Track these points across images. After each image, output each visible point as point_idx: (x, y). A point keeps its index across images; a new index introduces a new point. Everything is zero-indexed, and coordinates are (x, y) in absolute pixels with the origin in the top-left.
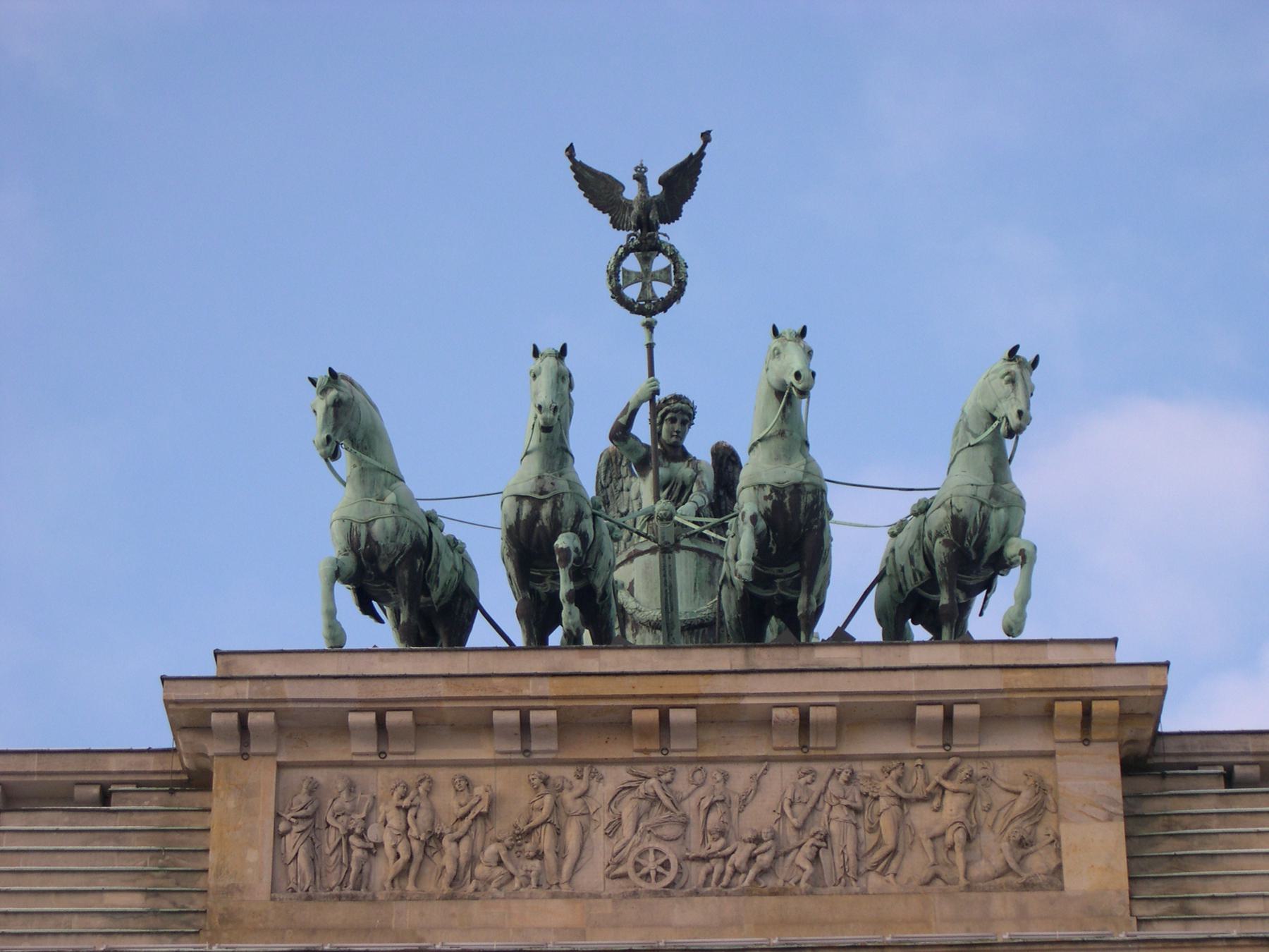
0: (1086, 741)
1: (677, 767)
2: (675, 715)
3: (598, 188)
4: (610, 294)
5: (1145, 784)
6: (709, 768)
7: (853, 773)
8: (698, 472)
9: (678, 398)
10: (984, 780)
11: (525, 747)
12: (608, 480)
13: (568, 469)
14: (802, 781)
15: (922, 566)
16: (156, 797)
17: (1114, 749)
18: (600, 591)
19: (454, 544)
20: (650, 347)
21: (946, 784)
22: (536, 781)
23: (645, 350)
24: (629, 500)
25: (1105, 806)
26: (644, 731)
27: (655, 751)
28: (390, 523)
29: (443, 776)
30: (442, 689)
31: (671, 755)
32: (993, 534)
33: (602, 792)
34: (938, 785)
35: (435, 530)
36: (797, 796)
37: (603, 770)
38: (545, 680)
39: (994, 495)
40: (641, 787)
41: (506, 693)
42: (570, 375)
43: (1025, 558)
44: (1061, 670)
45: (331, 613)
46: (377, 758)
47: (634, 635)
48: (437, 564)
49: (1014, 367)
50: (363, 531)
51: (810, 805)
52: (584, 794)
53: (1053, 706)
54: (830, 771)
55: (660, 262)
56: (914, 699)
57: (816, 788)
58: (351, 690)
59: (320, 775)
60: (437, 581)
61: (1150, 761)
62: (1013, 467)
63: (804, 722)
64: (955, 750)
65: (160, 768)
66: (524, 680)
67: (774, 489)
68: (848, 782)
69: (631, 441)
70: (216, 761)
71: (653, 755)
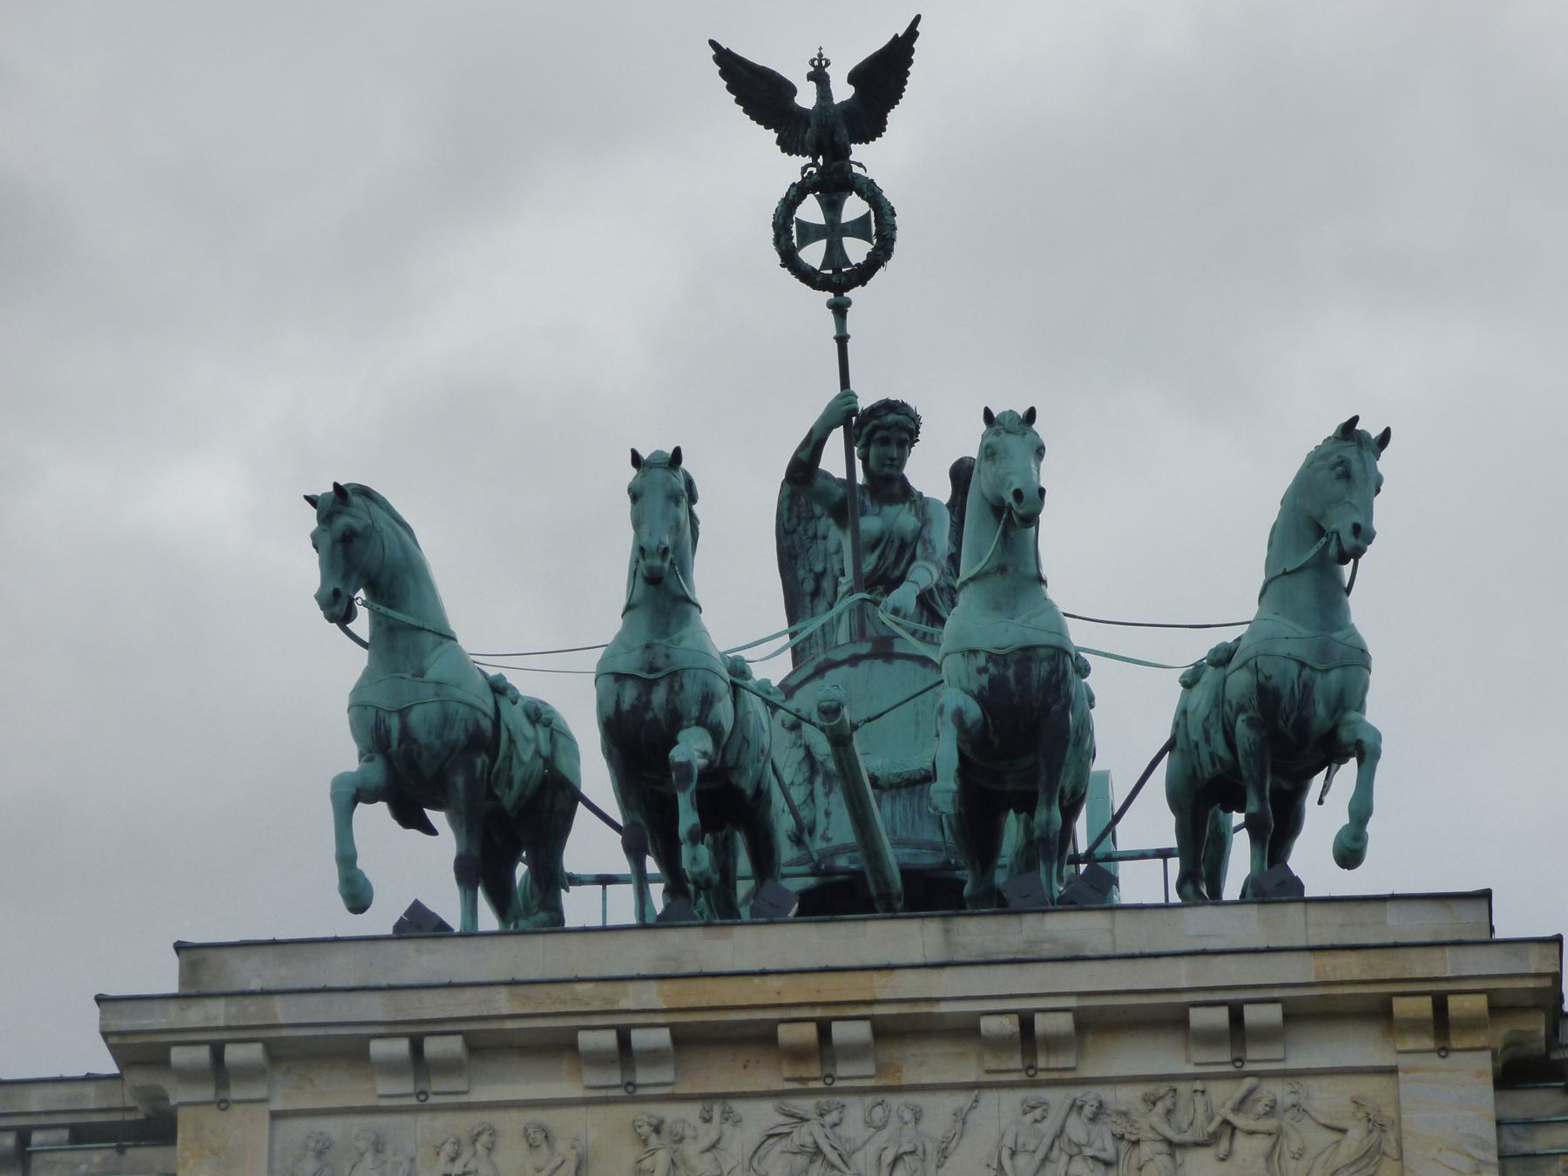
0: (1444, 1051)
1: (848, 1100)
2: (840, 1031)
3: (757, 90)
4: (778, 260)
5: (1539, 1101)
6: (895, 1101)
7: (1101, 1105)
8: (925, 522)
9: (889, 406)
10: (1293, 1112)
11: (628, 1079)
12: (794, 521)
13: (687, 631)
14: (1029, 1118)
15: (1221, 749)
16: (97, 1158)
17: (1484, 1062)
18: (749, 792)
19: (538, 715)
20: (842, 340)
21: (1238, 1120)
22: (646, 1130)
23: (835, 345)
24: (826, 555)
25: (1472, 1150)
26: (797, 1054)
27: (816, 1079)
28: (433, 710)
29: (512, 1123)
30: (503, 1003)
31: (838, 1084)
32: (1321, 710)
33: (740, 1141)
34: (1226, 1122)
35: (504, 704)
36: (1021, 1141)
37: (739, 1107)
38: (653, 985)
39: (1324, 651)
40: (795, 1135)
41: (596, 1005)
42: (690, 483)
43: (1366, 753)
44: (1400, 953)
45: (347, 860)
46: (413, 1101)
47: (827, 794)
48: (509, 758)
49: (1350, 452)
50: (394, 723)
51: (1040, 1155)
52: (713, 1146)
53: (1390, 1006)
54: (1069, 1102)
55: (854, 208)
56: (1185, 998)
57: (1048, 1128)
58: (374, 1008)
59: (333, 1128)
60: (510, 784)
61: (1555, 1056)
62: (1353, 600)
63: (1026, 1036)
64: (1249, 1067)
65: (104, 1105)
66: (620, 986)
67: (992, 657)
68: (1093, 1119)
69: (820, 482)
70: (182, 1114)
71: (813, 1085)
